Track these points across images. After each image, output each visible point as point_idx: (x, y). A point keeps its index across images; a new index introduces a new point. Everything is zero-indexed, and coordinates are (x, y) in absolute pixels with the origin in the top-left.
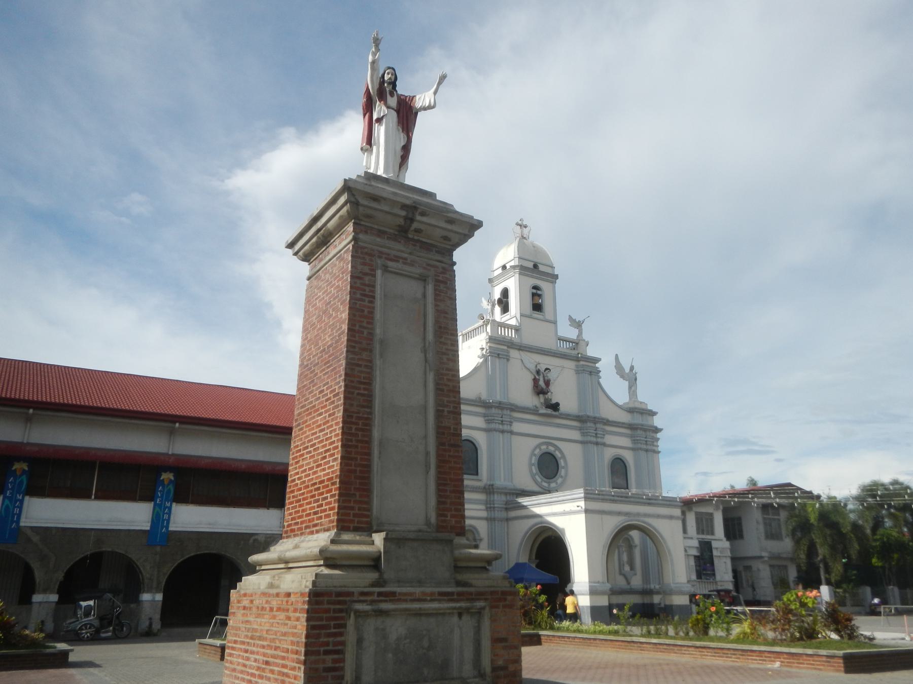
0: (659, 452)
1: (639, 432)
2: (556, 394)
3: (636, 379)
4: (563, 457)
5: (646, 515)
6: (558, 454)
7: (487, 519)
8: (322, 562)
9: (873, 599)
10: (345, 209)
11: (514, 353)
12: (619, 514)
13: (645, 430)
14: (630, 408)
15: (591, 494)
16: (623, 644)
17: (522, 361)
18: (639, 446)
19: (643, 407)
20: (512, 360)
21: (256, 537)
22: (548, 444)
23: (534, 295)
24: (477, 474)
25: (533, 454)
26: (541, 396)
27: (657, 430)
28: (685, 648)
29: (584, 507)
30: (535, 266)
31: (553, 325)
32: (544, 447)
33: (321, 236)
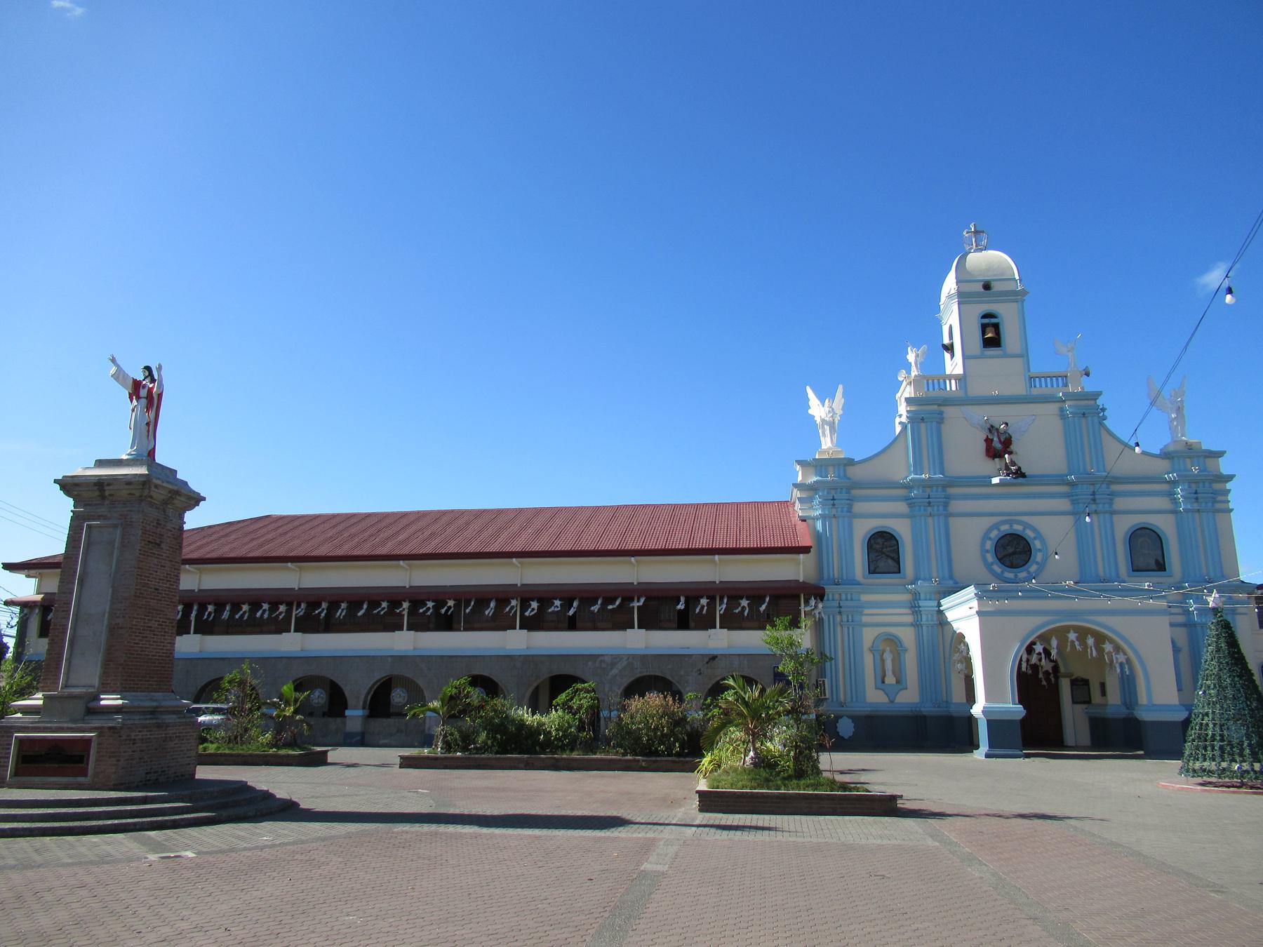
2: (1027, 454)
4: (1039, 536)
6: (1029, 534)
7: (912, 625)
11: (949, 411)
17: (965, 418)
21: (602, 658)
22: (1011, 523)
23: (984, 328)
24: (900, 572)
25: (986, 537)
26: (997, 460)
29: (976, 608)
30: (987, 286)
31: (1020, 360)
32: (1005, 528)
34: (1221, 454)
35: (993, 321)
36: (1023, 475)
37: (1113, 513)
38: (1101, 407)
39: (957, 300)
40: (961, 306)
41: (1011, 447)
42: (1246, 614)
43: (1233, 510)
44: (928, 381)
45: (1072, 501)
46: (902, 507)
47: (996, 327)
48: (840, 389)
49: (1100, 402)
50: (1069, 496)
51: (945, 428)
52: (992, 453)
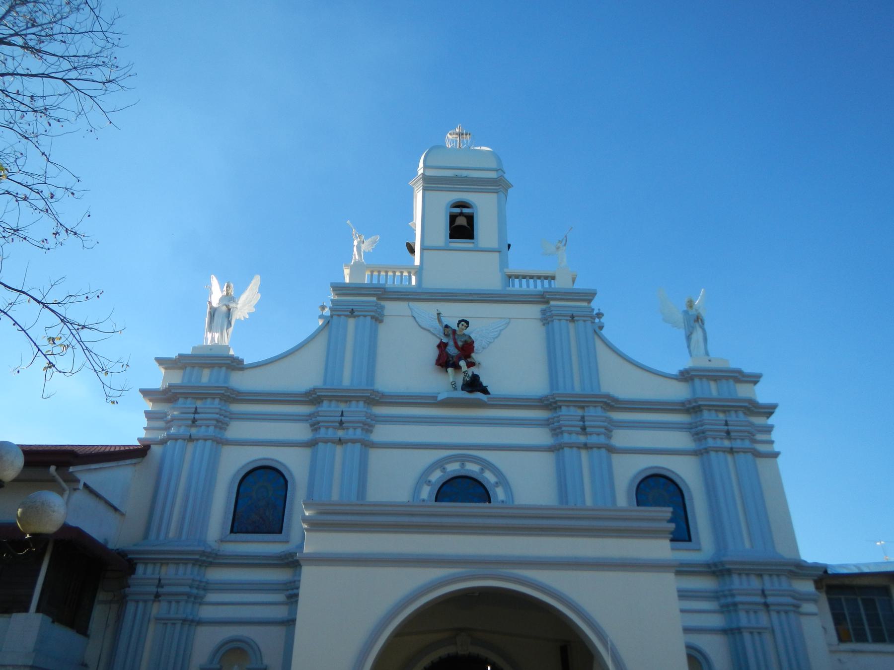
4: (503, 481)
6: (489, 478)
11: (391, 308)
20: (386, 319)
22: (463, 459)
23: (453, 218)
24: (280, 532)
25: (423, 479)
26: (450, 370)
32: (453, 468)
34: (754, 379)
35: (465, 210)
36: (485, 391)
37: (611, 450)
38: (596, 311)
39: (422, 188)
40: (427, 193)
41: (473, 355)
42: (815, 614)
44: (372, 272)
45: (554, 430)
46: (300, 431)
47: (470, 219)
48: (256, 281)
49: (596, 304)
50: (548, 425)
51: (383, 329)
52: (445, 362)
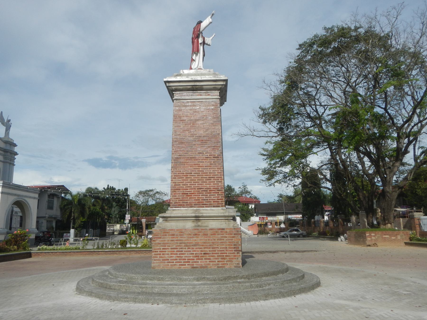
0: (15, 165)
1: (9, 154)
3: (11, 126)
5: (26, 197)
8: (232, 218)
9: (86, 234)
10: (220, 86)
12: (15, 195)
13: (11, 153)
14: (6, 141)
15: (8, 185)
16: (88, 253)
18: (8, 161)
19: (12, 141)
27: (16, 154)
28: (122, 252)
33: (195, 88)
43: (15, 165)
